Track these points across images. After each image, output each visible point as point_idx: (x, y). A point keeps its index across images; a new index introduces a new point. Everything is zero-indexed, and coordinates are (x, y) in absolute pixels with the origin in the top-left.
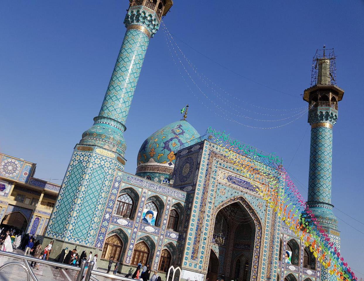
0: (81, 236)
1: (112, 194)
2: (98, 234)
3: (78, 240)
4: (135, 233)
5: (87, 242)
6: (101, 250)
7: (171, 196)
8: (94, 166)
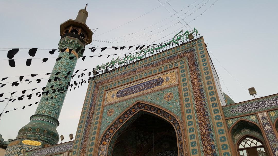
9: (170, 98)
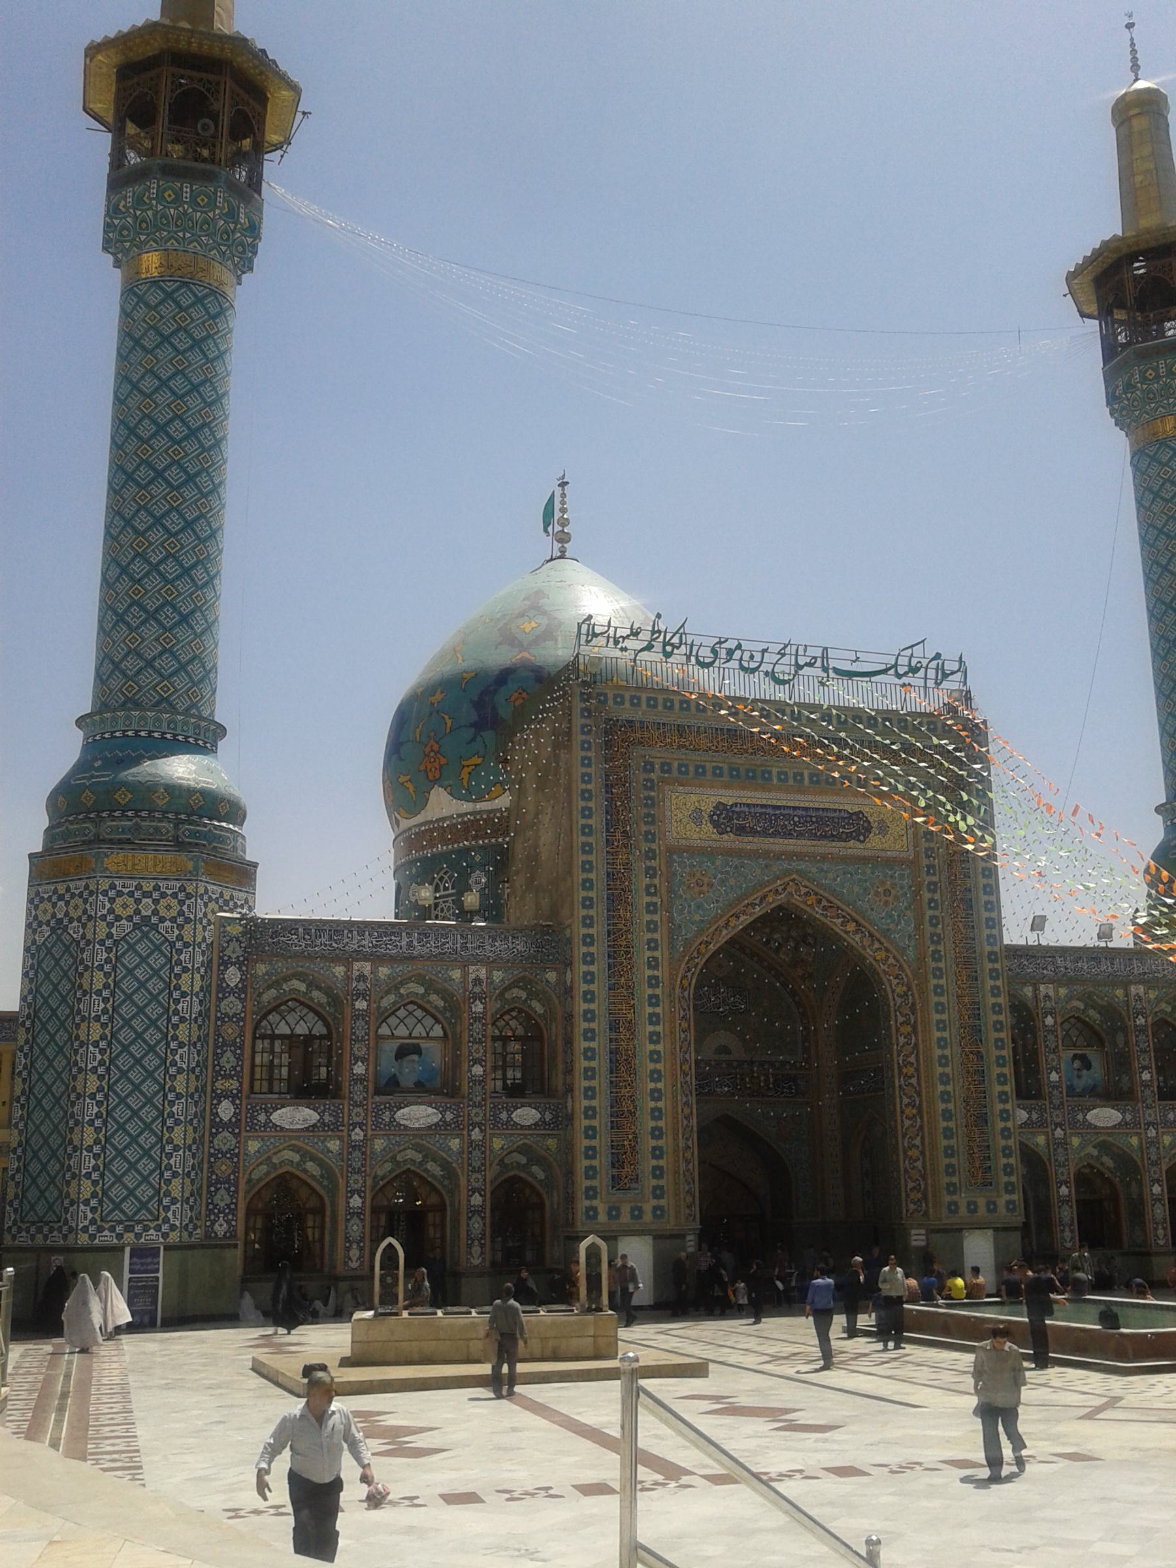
0: (136, 1214)
1: (223, 1018)
2: (205, 1187)
3: (129, 1229)
5: (165, 1228)
6: (236, 1246)
7: (478, 961)
8: (113, 930)
9: (890, 899)
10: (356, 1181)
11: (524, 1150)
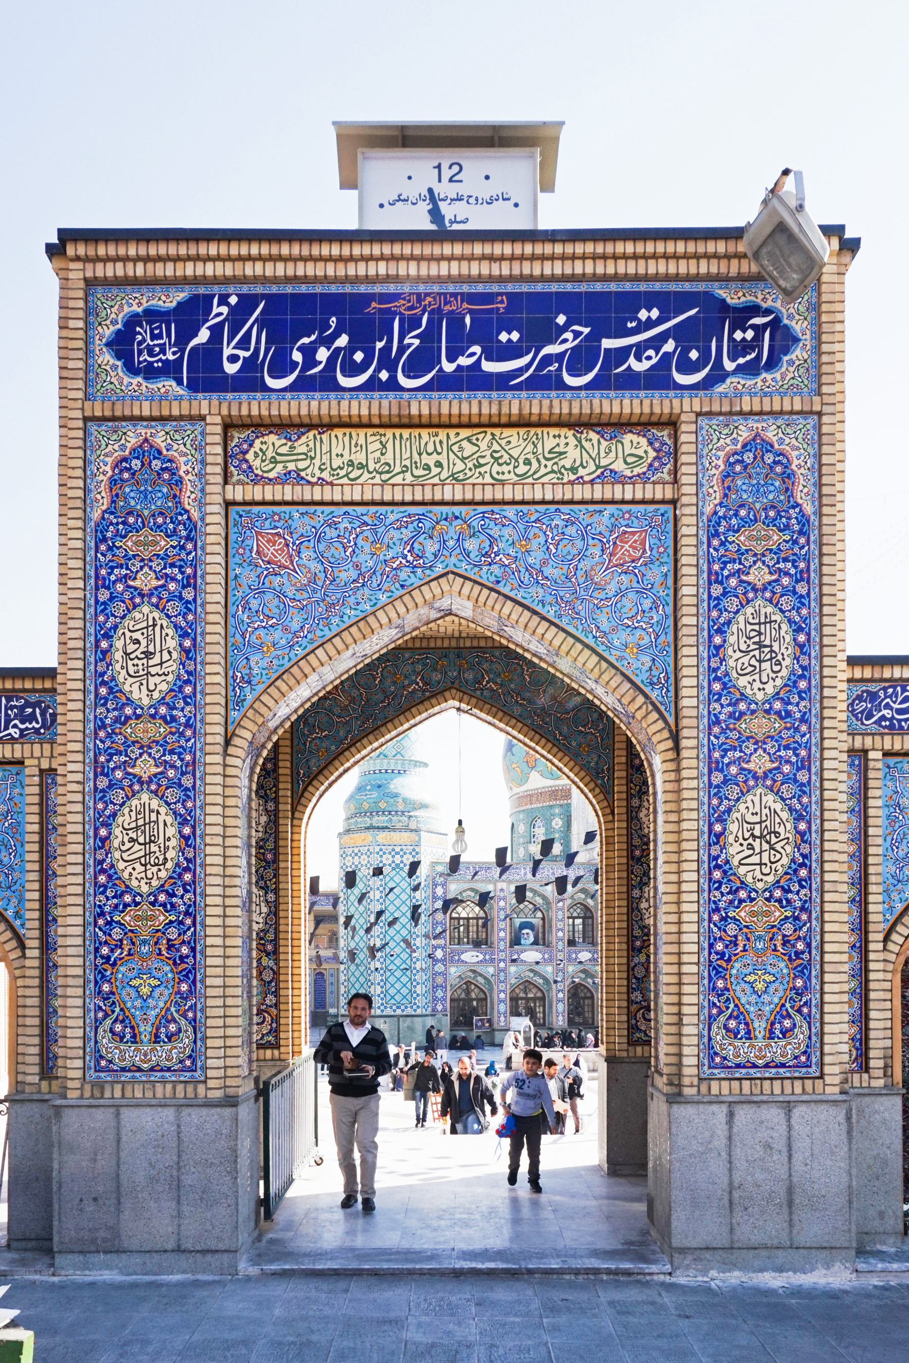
3: (398, 1008)
4: (504, 970)
10: (502, 986)
11: (584, 971)
